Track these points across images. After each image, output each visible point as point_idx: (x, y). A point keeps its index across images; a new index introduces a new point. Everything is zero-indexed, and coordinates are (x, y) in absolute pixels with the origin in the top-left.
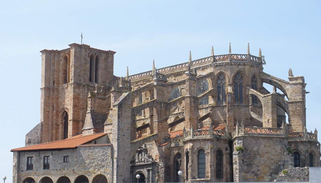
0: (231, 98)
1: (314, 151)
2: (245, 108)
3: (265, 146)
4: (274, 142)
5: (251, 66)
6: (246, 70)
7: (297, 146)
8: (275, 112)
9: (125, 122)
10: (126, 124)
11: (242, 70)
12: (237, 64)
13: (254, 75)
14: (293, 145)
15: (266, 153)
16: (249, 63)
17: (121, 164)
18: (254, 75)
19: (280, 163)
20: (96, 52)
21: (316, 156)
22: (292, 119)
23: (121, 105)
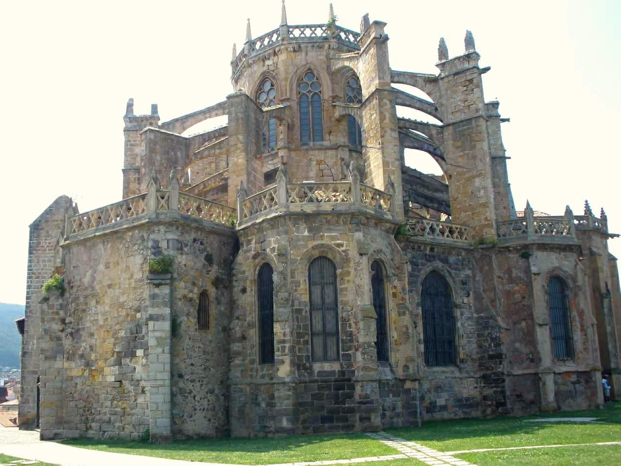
0: (146, 145)
1: (342, 245)
2: (272, 160)
5: (295, 51)
6: (281, 67)
8: (240, 145)
9: (46, 259)
10: (49, 263)
11: (272, 68)
13: (309, 69)
14: (254, 241)
15: (110, 286)
16: (282, 44)
17: (32, 349)
18: (309, 69)
19: (138, 315)
21: (352, 264)
23: (38, 225)
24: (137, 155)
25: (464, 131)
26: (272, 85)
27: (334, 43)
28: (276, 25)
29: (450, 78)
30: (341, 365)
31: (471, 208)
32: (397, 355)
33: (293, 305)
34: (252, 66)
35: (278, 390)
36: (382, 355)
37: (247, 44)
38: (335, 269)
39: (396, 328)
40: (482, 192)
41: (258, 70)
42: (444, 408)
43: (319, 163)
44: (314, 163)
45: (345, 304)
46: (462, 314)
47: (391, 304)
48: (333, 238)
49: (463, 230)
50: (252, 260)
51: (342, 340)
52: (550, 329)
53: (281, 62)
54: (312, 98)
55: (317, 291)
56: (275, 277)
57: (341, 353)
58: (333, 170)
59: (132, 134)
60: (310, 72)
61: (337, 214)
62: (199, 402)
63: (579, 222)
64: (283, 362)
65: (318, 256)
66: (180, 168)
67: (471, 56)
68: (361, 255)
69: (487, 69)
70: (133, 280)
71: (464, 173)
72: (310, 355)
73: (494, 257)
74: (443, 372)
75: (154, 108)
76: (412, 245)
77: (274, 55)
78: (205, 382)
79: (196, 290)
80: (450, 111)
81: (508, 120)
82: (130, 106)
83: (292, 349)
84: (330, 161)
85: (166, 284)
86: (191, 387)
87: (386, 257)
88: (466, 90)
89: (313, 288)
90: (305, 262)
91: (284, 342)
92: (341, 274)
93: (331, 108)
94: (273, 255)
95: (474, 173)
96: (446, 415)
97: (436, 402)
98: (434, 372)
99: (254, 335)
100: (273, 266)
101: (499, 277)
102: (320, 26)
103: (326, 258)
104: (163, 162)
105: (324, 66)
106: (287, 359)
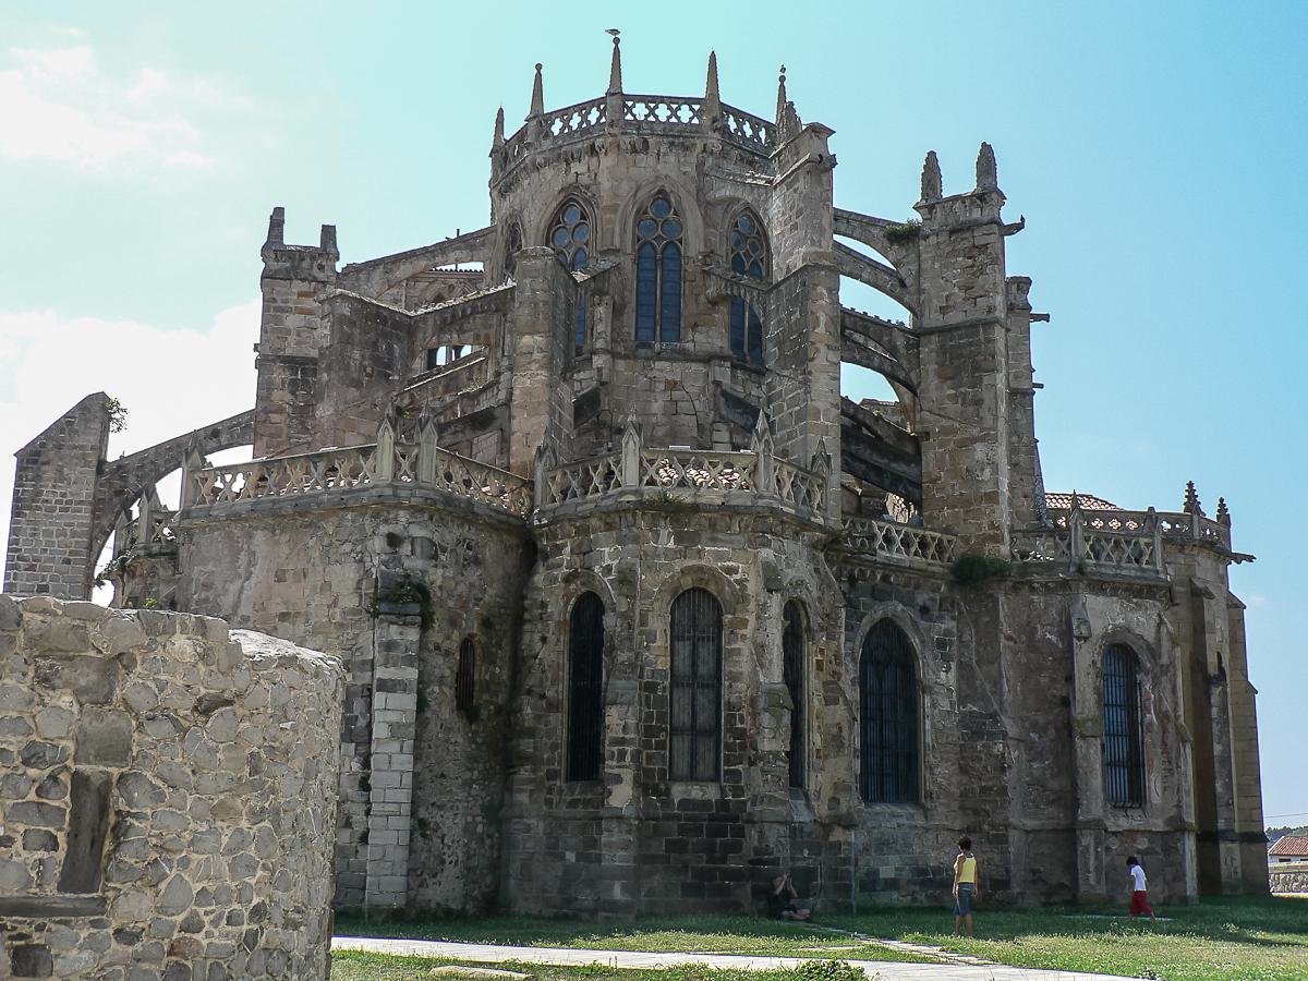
0: (332, 326)
3: (280, 577)
4: (326, 541)
5: (634, 150)
6: (603, 178)
7: (587, 549)
11: (584, 180)
12: (559, 155)
13: (661, 191)
14: (568, 549)
20: (453, 281)
21: (752, 606)
22: (778, 389)
23: (38, 454)
24: (288, 331)
25: (961, 346)
26: (583, 217)
27: (714, 140)
28: (600, 91)
29: (941, 239)
30: (722, 790)
31: (966, 502)
32: (820, 778)
33: (641, 677)
34: (542, 171)
35: (609, 831)
36: (796, 780)
37: (534, 122)
38: (720, 614)
39: (819, 727)
40: (988, 470)
41: (553, 180)
42: (892, 884)
43: (672, 385)
44: (662, 386)
45: (735, 678)
46: (934, 705)
47: (813, 683)
48: (720, 557)
49: (946, 543)
50: (563, 585)
51: (726, 743)
52: (1103, 745)
53: (606, 171)
54: (662, 253)
55: (684, 649)
56: (609, 621)
57: (723, 767)
58: (696, 403)
59: (281, 286)
60: (662, 195)
61: (728, 510)
62: (449, 847)
63: (1173, 526)
64: (618, 779)
65: (691, 587)
66: (396, 378)
67: (988, 193)
68: (770, 591)
69: (1019, 227)
70: (337, 610)
71: (954, 431)
72: (667, 768)
73: (1002, 599)
74: (894, 815)
75: (328, 233)
76: (849, 568)
77: (592, 154)
78: (461, 811)
79: (456, 636)
80: (936, 303)
81: (1046, 318)
82: (277, 220)
83: (636, 756)
84: (693, 387)
85: (413, 624)
86: (438, 819)
87: (811, 592)
88: (972, 266)
89: (679, 645)
90: (667, 598)
91: (622, 741)
92: (731, 623)
93: (699, 277)
94: (606, 579)
95: (975, 432)
96: (895, 897)
97: (877, 872)
98: (877, 814)
99: (559, 723)
100: (605, 600)
101: (1009, 638)
102: (689, 101)
103: (705, 591)
104: (366, 363)
105: (692, 187)
106: (628, 775)
